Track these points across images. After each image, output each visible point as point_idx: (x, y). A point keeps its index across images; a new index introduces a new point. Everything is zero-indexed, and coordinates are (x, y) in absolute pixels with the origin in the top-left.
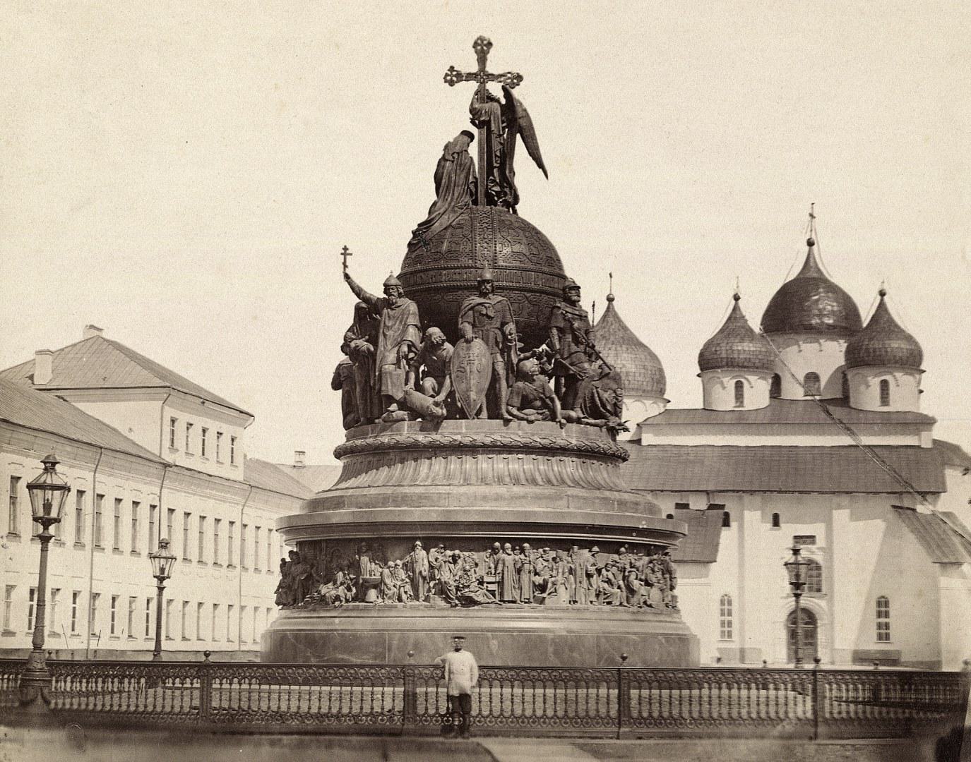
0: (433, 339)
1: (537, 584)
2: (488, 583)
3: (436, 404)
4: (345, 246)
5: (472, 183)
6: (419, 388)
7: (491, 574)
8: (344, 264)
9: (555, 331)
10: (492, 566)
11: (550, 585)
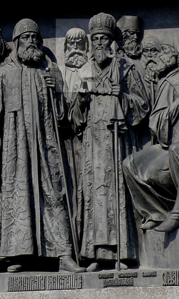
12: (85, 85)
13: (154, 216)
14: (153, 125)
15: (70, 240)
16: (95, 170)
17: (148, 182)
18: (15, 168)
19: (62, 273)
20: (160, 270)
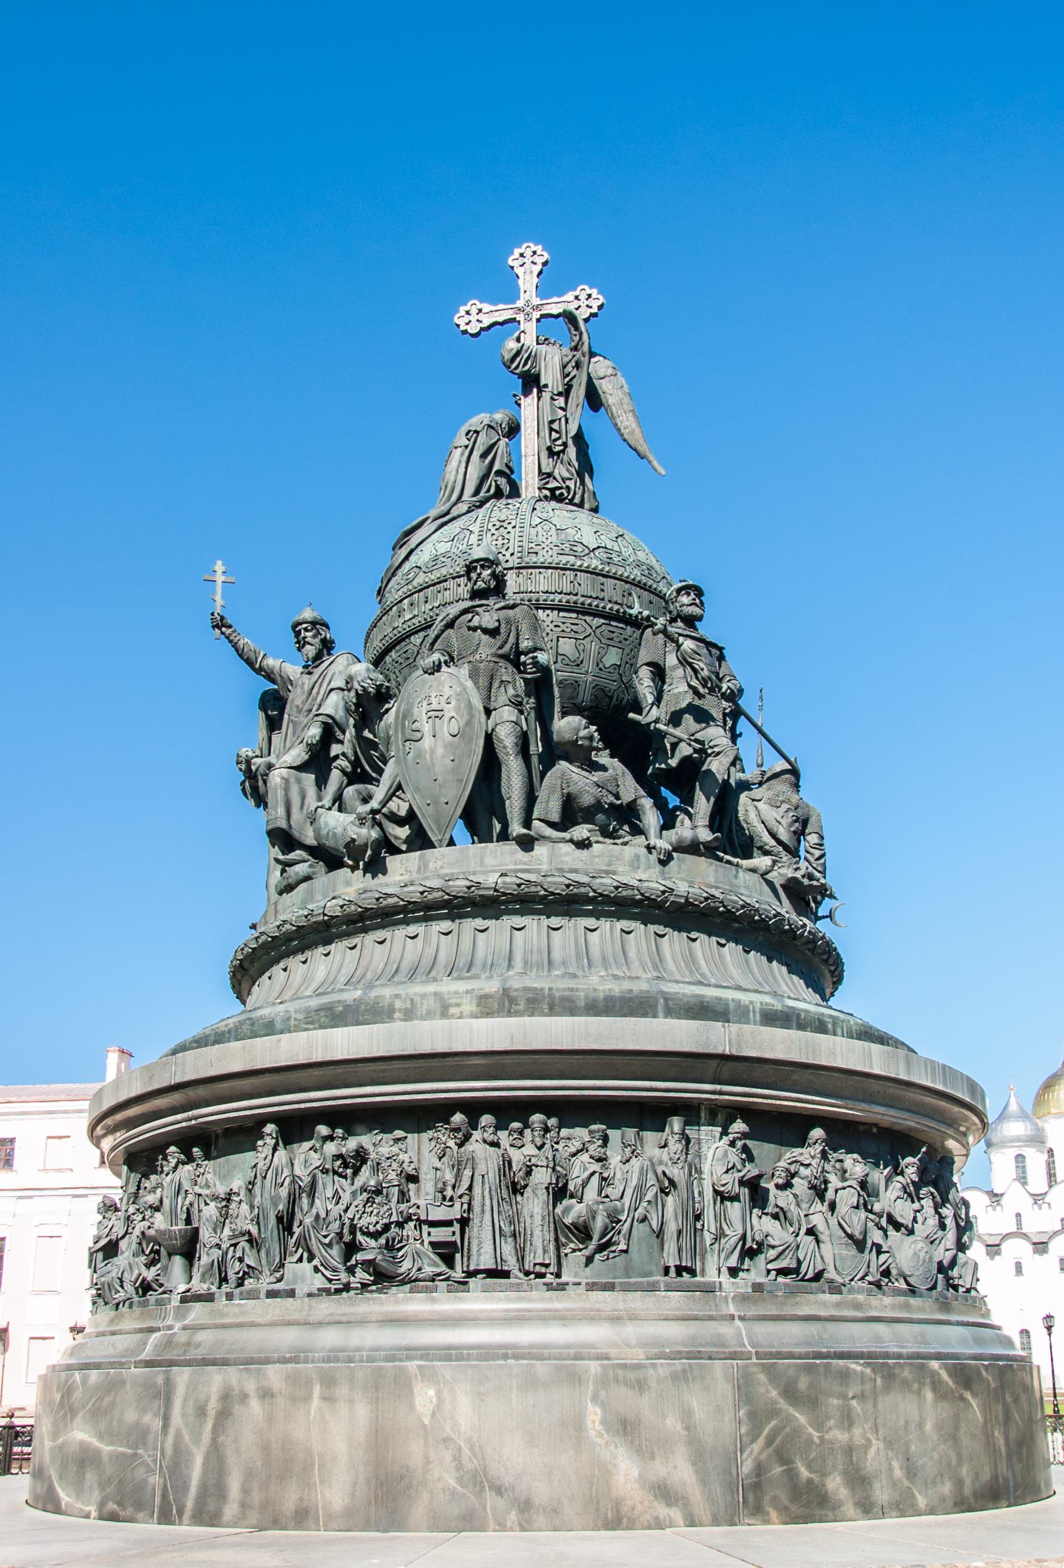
5: (499, 473)
6: (339, 801)
7: (444, 1198)
9: (645, 673)
10: (449, 1177)
12: (530, 1160)
13: (572, 1245)
14: (571, 1187)
15: (518, 1260)
16: (535, 1215)
17: (572, 1224)
18: (483, 1211)
19: (512, 1280)
20: (584, 1281)
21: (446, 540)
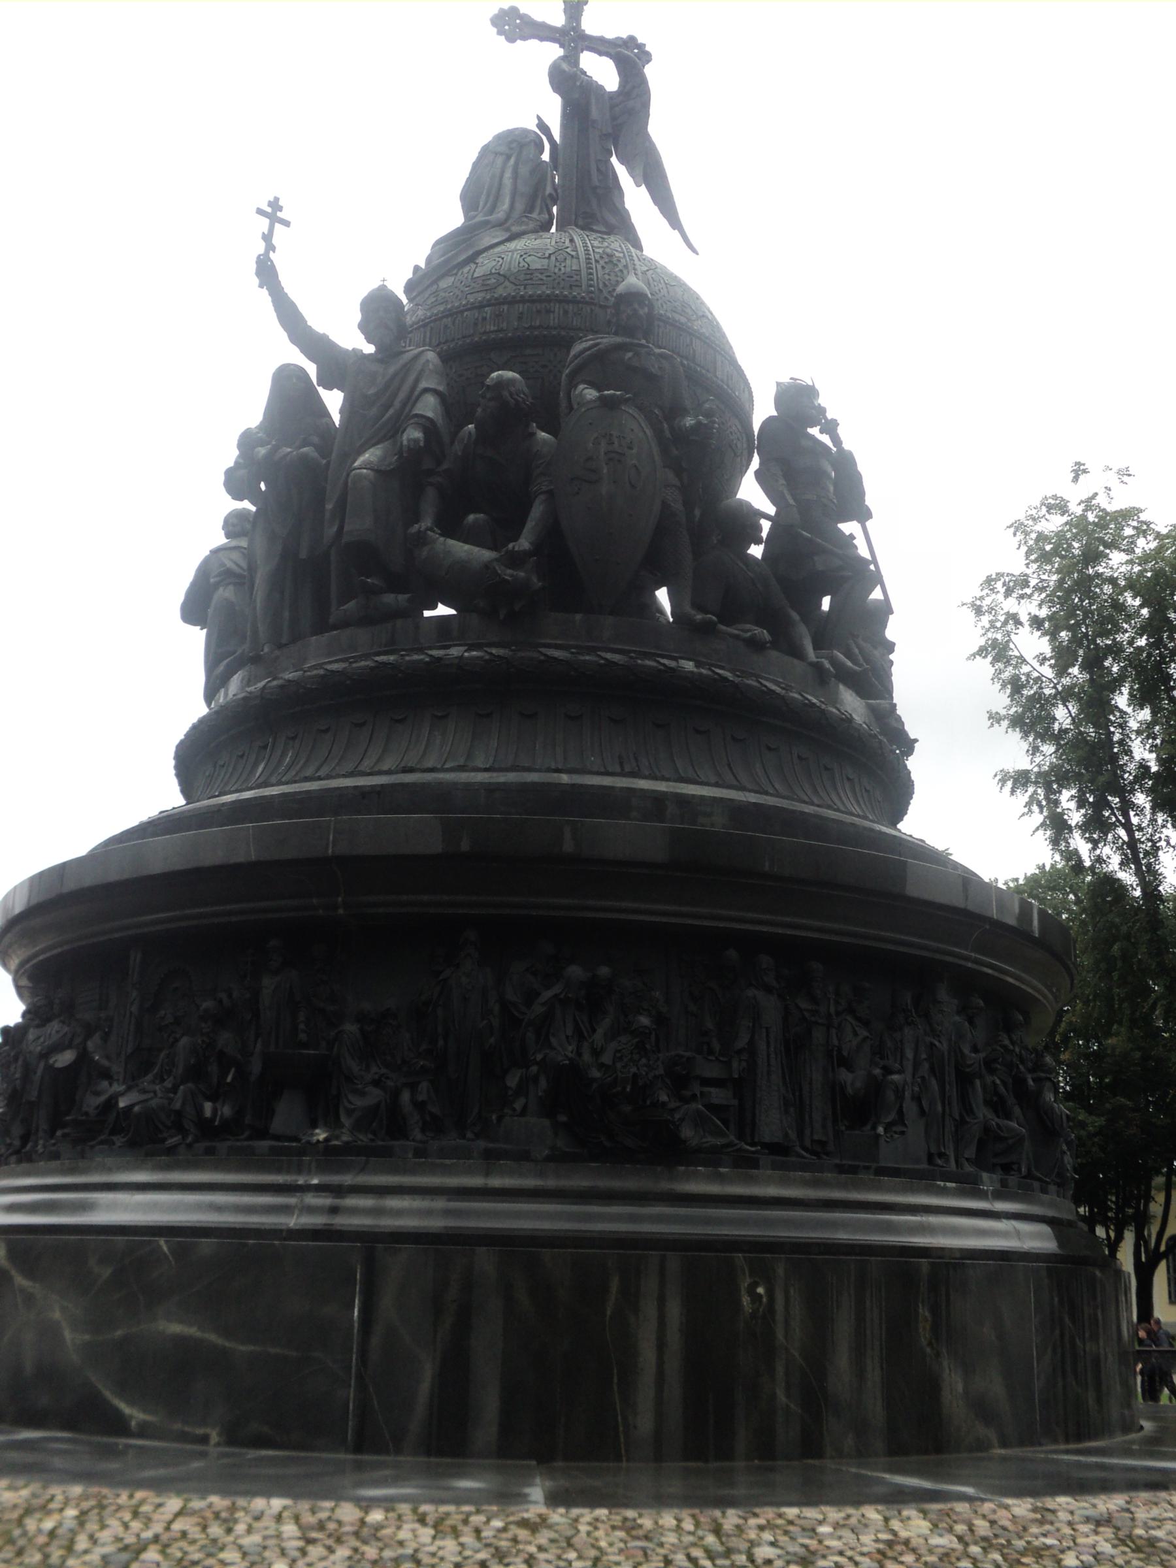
0: (506, 393)
1: (850, 1091)
2: (706, 1082)
3: (515, 560)
4: (277, 199)
8: (267, 238)
10: (709, 1024)
11: (890, 1096)
21: (539, 255)
